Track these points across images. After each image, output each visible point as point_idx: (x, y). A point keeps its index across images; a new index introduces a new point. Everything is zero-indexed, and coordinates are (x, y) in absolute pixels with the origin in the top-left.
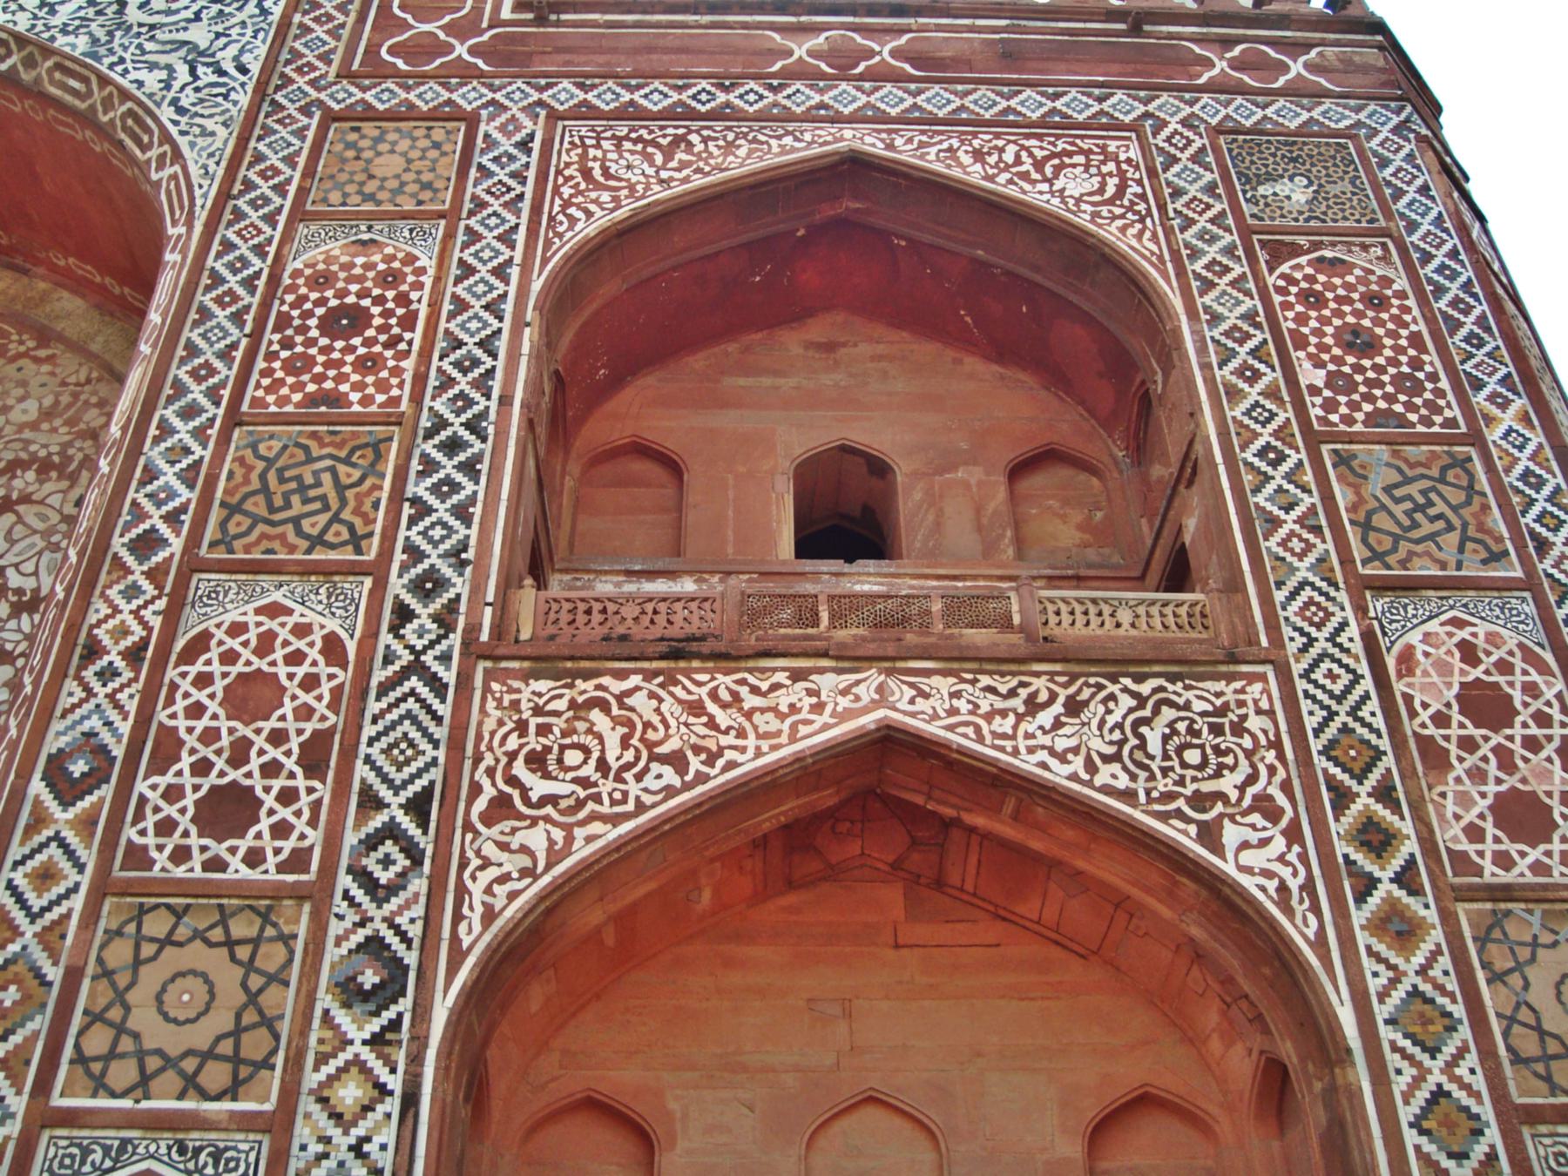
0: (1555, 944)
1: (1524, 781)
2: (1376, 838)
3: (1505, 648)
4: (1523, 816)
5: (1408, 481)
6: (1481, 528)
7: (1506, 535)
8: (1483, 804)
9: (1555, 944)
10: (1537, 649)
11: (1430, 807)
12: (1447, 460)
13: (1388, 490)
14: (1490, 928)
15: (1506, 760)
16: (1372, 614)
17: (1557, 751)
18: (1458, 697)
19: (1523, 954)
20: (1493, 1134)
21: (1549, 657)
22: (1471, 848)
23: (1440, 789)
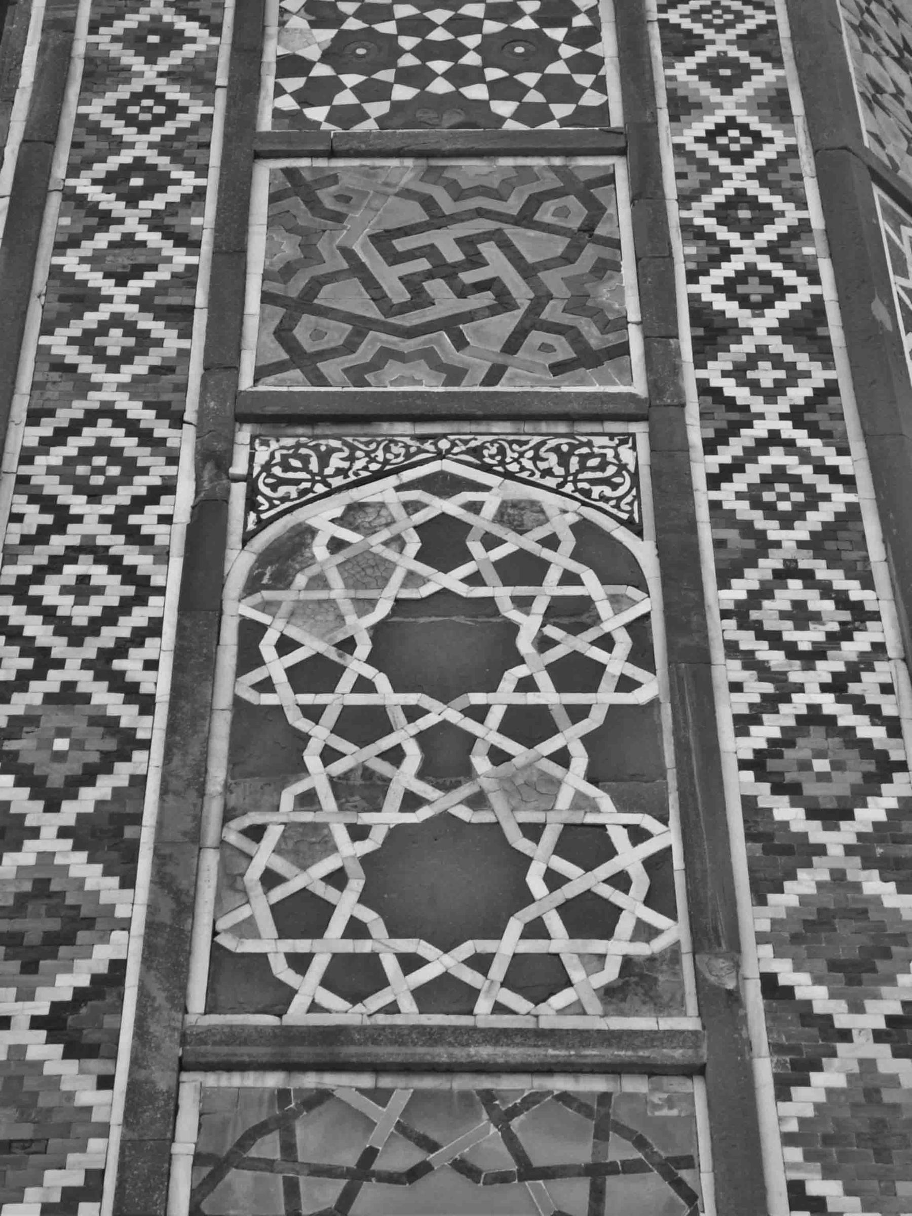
1: (478, 801)
2: (35, 926)
3: (542, 532)
4: (447, 881)
5: (438, 220)
6: (579, 303)
7: (634, 315)
8: (349, 851)
10: (622, 535)
11: (210, 860)
12: (552, 182)
13: (382, 240)
14: (261, 1130)
15: (446, 757)
16: (239, 467)
17: (587, 740)
18: (377, 632)
21: (645, 552)
22: (274, 948)
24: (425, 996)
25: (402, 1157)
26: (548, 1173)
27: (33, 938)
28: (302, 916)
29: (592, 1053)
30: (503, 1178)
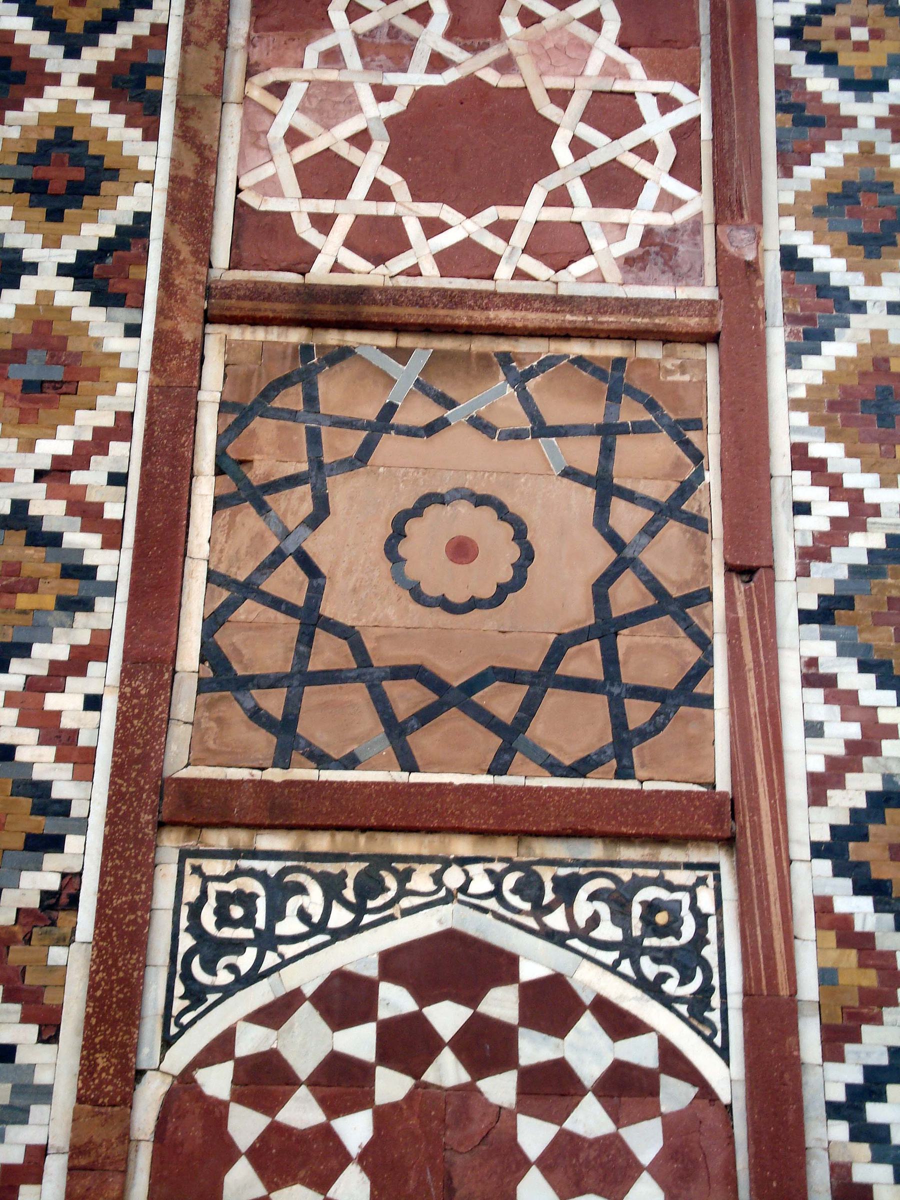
0: (432, 429)
1: (506, 65)
8: (373, 113)
9: (432, 429)
11: (233, 116)
14: (284, 382)
19: (341, 444)
20: (85, 852)
22: (299, 209)
23: (277, 74)
24: (447, 261)
25: (422, 412)
26: (559, 432)
27: (57, 186)
28: (326, 176)
29: (609, 320)
30: (517, 435)
